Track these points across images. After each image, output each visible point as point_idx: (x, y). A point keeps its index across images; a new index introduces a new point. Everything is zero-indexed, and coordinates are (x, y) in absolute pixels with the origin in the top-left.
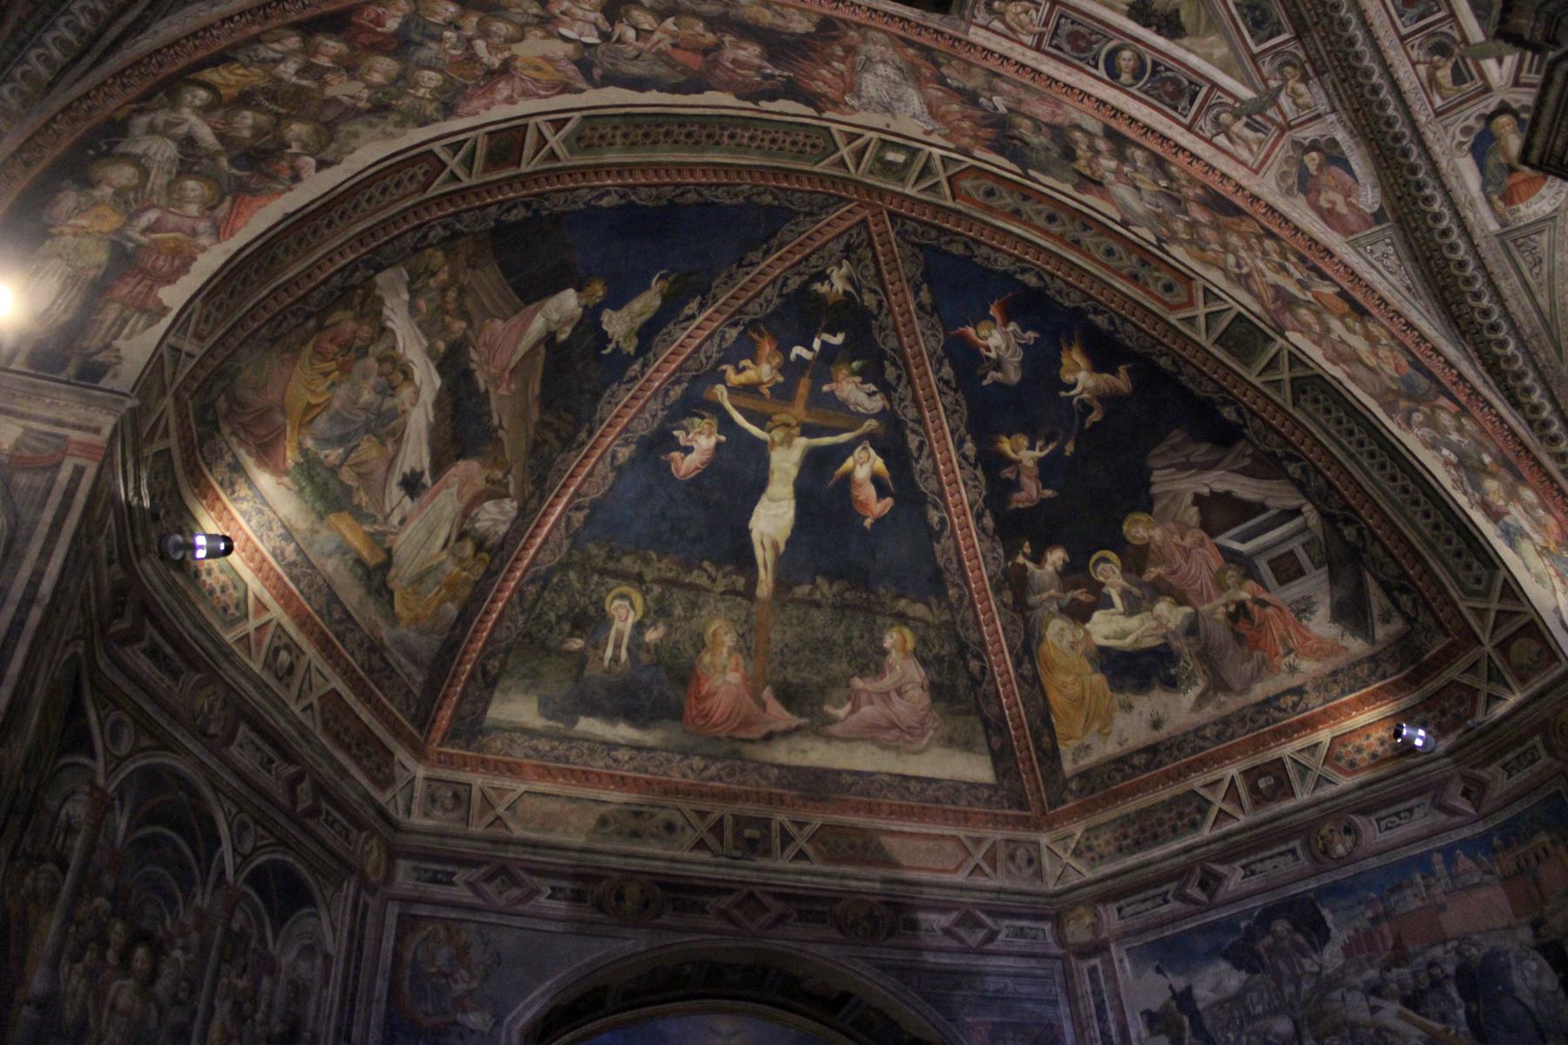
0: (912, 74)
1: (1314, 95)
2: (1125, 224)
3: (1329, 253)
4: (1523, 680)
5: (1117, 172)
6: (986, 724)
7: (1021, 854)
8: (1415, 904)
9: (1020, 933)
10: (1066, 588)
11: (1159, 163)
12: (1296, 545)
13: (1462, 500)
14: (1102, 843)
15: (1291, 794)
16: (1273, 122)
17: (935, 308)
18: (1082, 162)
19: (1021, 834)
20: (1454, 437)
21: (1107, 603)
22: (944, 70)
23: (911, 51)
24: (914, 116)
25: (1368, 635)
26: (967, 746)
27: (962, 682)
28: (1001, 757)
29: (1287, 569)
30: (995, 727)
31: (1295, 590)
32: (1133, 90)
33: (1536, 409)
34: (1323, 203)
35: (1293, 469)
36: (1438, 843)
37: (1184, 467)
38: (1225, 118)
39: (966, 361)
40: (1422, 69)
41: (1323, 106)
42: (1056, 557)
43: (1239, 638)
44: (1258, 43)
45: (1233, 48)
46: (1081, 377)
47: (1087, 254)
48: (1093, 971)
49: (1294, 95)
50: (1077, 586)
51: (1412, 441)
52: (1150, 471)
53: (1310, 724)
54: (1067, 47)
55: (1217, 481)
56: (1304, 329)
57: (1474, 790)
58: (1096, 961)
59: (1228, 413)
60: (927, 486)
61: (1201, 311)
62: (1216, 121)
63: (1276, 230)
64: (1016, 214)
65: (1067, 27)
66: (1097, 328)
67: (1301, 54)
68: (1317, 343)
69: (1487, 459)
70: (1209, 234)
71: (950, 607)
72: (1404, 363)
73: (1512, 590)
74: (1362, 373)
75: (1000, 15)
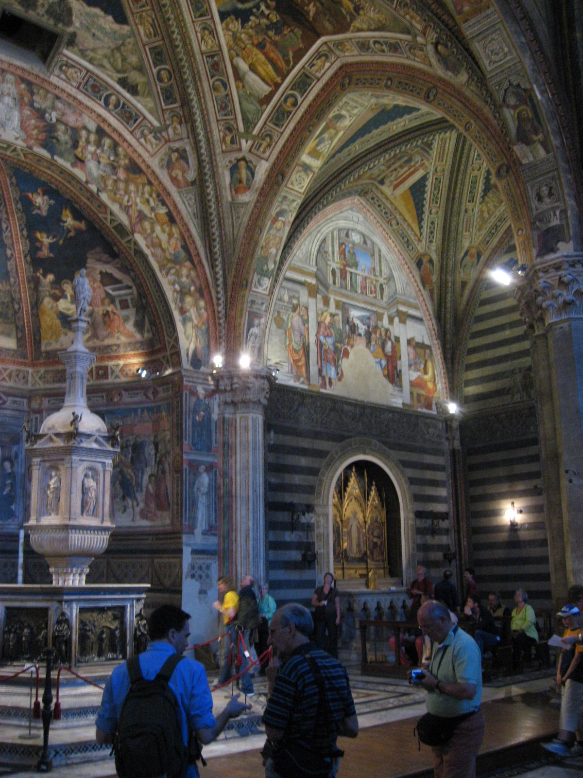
0: (20, 102)
1: (182, 130)
2: (87, 182)
3: (169, 194)
4: (173, 368)
5: (94, 154)
6: (17, 328)
7: (21, 375)
8: (129, 422)
9: (15, 402)
10: (52, 288)
11: (115, 146)
12: (129, 298)
13: (173, 306)
14: (49, 377)
15: (107, 378)
16: (164, 137)
17: (17, 185)
18: (80, 149)
19: (23, 368)
20: (184, 279)
21: (66, 297)
22: (35, 98)
23: (23, 86)
24: (14, 129)
25: (142, 334)
26: (8, 335)
27: (11, 312)
28: (20, 341)
29: (124, 305)
30: (20, 329)
31: (125, 312)
32: (113, 113)
33: (216, 273)
34: (174, 174)
35: (132, 274)
36: (142, 406)
37: (99, 260)
38: (146, 132)
39: (27, 205)
40: (222, 134)
41: (185, 135)
42: (51, 277)
43: (105, 323)
44: (166, 105)
45: (156, 105)
46: (69, 221)
47: (73, 186)
48: (36, 419)
49: (175, 129)
50: (56, 289)
51: (165, 283)
52: (87, 258)
53: (118, 357)
54: (90, 90)
55: (109, 269)
56: (143, 232)
57: (155, 393)
58: (38, 416)
59: (115, 249)
60: (8, 242)
61: (109, 217)
62: (142, 132)
63: (153, 181)
64: (49, 168)
65: (91, 82)
66: (76, 208)
67: (181, 113)
68: (145, 239)
69: (192, 289)
70: (121, 185)
71: (11, 285)
72: (179, 246)
73: (177, 340)
74: (159, 252)
75: (65, 73)
